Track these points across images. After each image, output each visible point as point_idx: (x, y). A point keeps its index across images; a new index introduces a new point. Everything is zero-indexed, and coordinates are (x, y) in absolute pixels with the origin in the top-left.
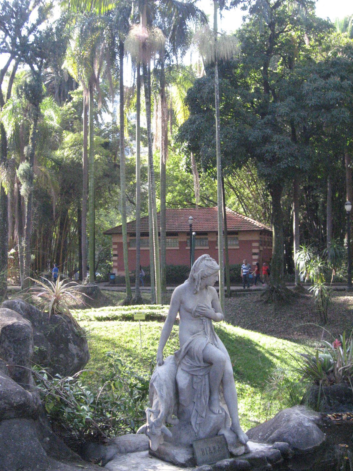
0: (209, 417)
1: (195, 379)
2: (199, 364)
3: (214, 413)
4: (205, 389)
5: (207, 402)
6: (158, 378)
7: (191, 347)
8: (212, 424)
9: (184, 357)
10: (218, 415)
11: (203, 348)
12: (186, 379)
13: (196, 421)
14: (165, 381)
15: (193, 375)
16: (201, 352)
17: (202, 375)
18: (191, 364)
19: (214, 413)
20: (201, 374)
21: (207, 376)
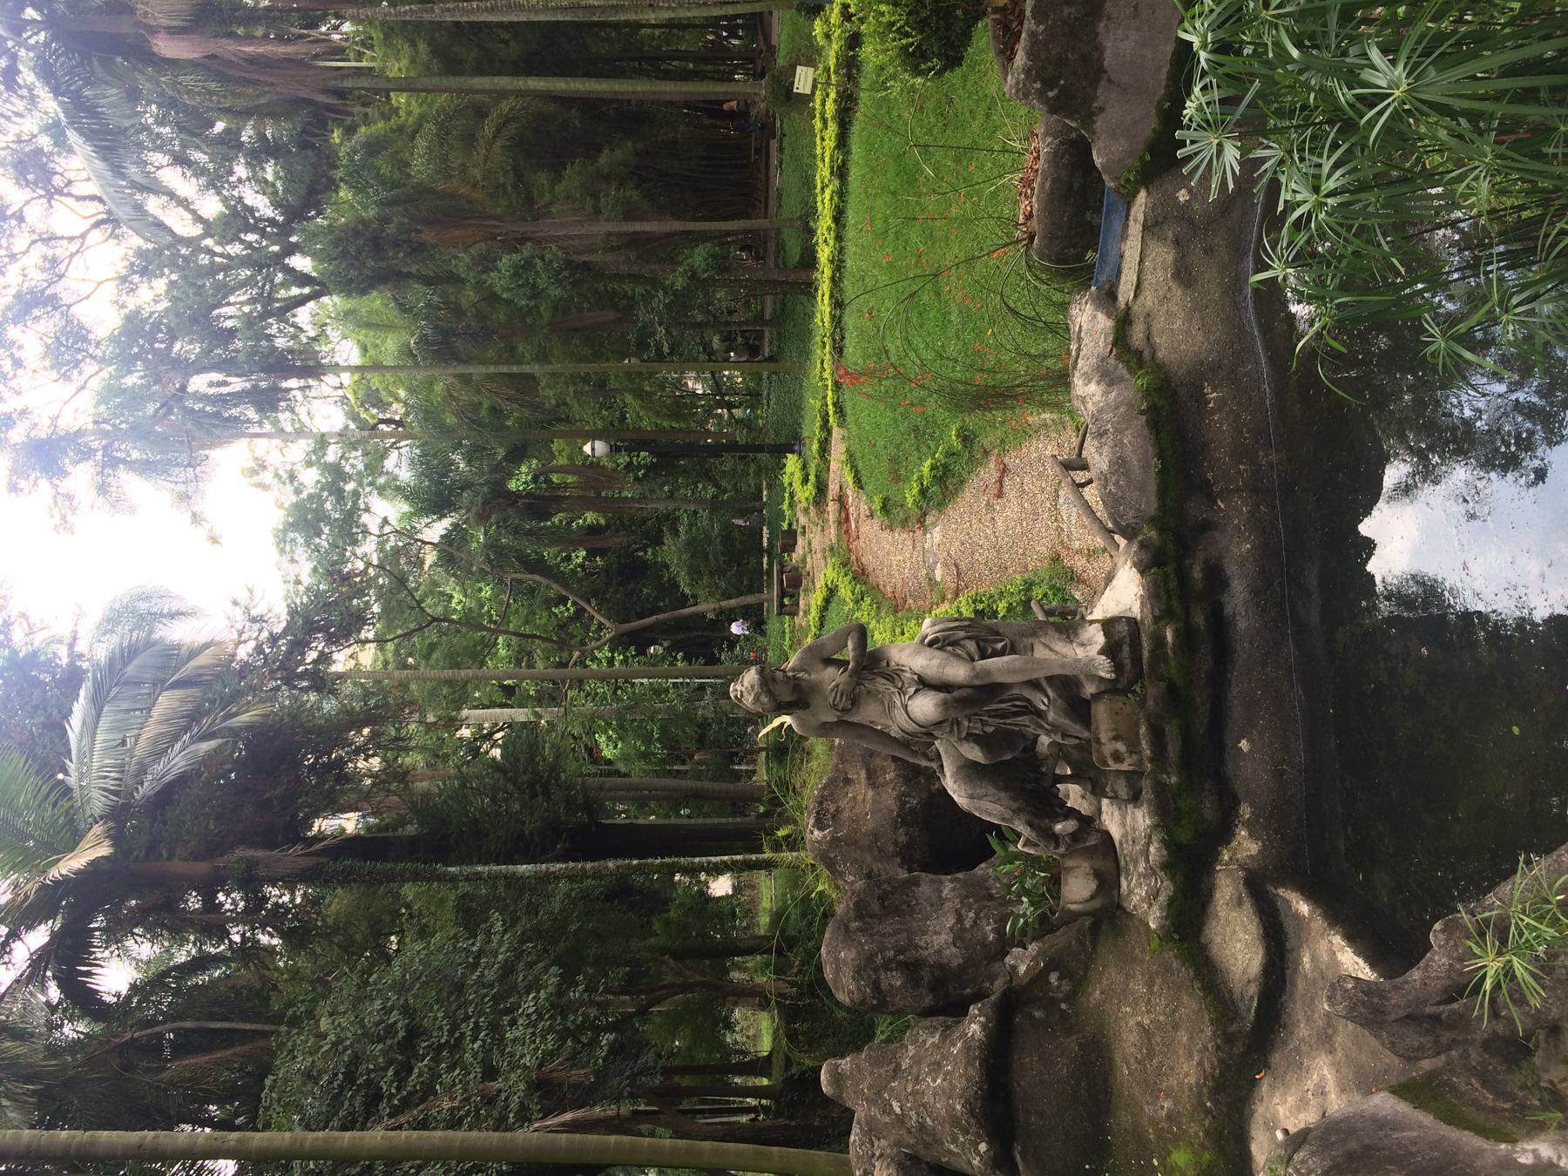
14: (971, 797)
15: (969, 735)
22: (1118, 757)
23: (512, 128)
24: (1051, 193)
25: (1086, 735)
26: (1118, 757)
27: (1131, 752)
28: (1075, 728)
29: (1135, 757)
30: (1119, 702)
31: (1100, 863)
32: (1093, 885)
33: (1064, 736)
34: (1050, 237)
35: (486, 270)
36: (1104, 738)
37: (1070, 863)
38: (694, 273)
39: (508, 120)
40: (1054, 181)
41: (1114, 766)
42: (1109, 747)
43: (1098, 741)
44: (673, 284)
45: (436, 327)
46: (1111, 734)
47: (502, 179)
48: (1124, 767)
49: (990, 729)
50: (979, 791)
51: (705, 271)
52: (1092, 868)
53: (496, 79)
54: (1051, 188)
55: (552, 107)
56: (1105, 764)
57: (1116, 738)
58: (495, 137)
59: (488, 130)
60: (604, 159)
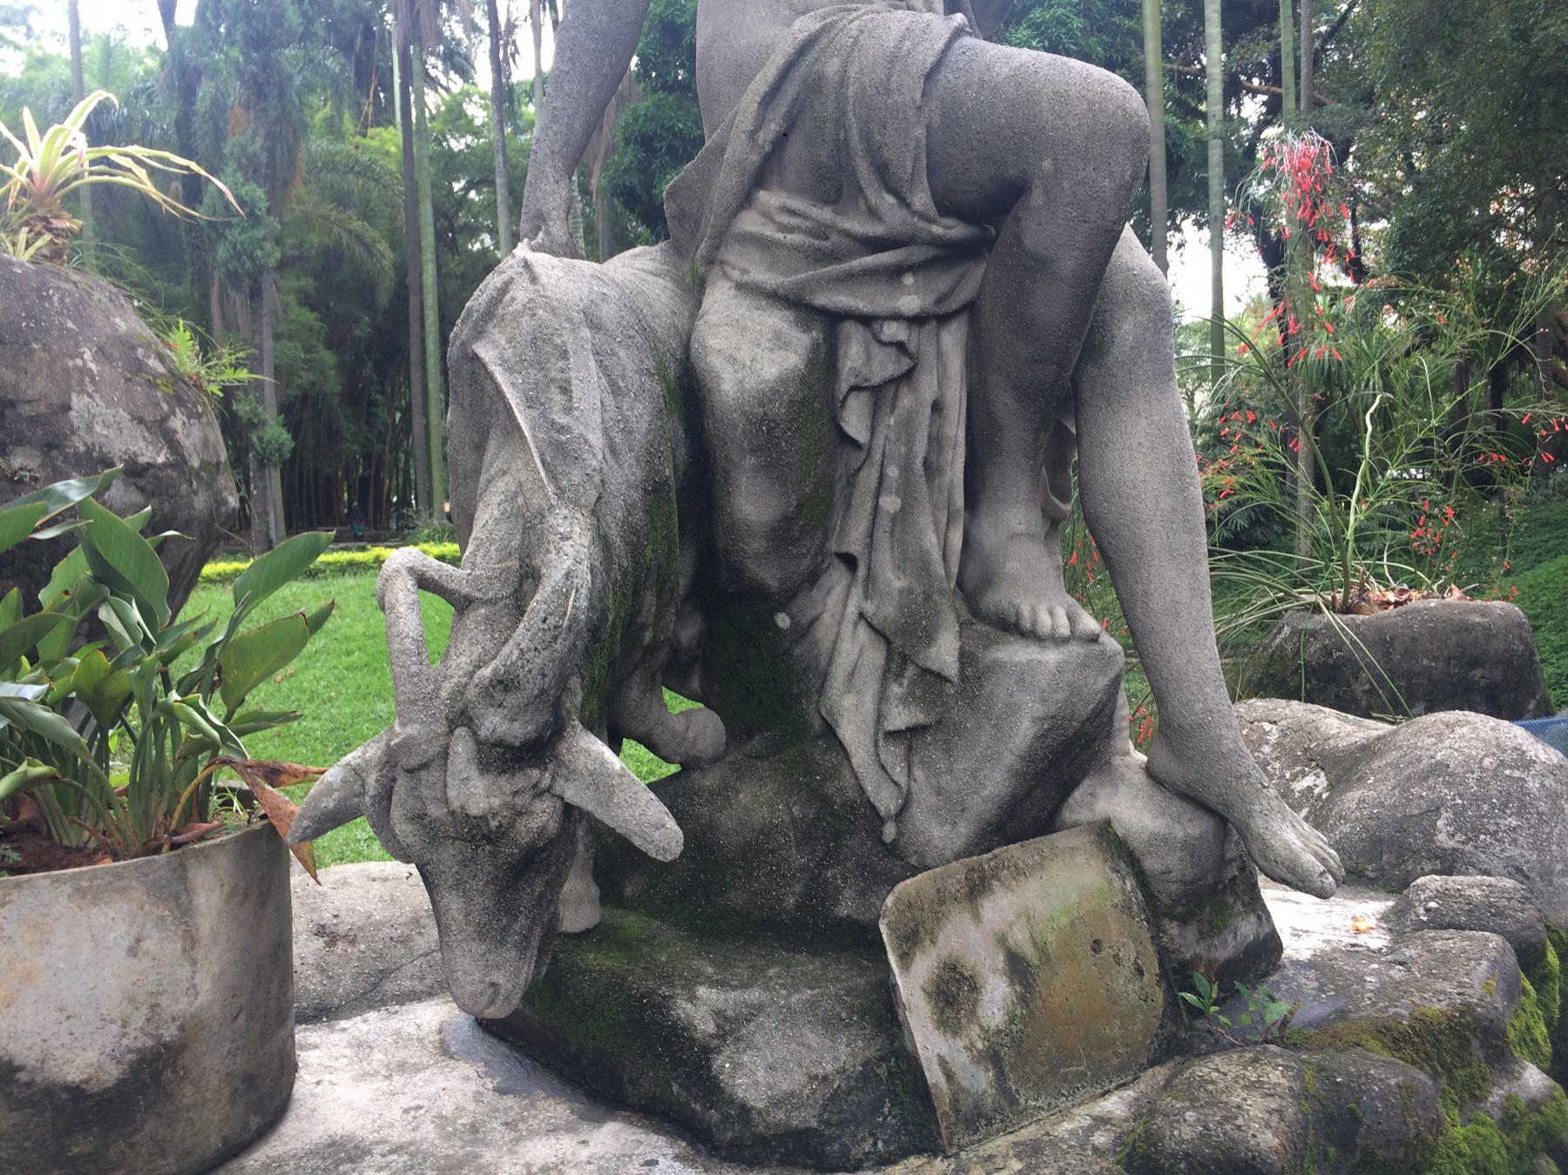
0: (997, 666)
1: (855, 354)
2: (893, 217)
3: (1032, 635)
4: (936, 442)
5: (955, 570)
6: (521, 293)
7: (815, 85)
8: (1024, 731)
9: (745, 201)
10: (1075, 650)
11: (926, 55)
12: (778, 341)
13: (880, 718)
15: (833, 320)
16: (912, 89)
17: (916, 321)
18: (820, 231)
19: (1032, 635)
20: (910, 303)
21: (953, 339)
22: (952, 994)
23: (359, 250)
24: (1468, 628)
25: (938, 832)
26: (952, 994)
27: (992, 1057)
28: (989, 772)
29: (980, 1080)
30: (1129, 943)
31: (213, 1065)
32: (84, 1057)
33: (909, 736)
34: (1383, 641)
35: (240, 167)
36: (999, 908)
37: (209, 892)
38: (254, 426)
39: (368, 247)
40: (1486, 629)
41: (912, 985)
42: (969, 938)
43: (977, 889)
44: (238, 401)
45: (120, 126)
46: (1020, 938)
47: (289, 242)
48: (928, 1041)
49: (855, 423)
50: (627, 360)
51: (261, 440)
52: (191, 1028)
53: (431, 229)
54: (1474, 626)
55: (383, 298)
56: (911, 941)
57: (1017, 966)
58: (350, 232)
59: (357, 225)
60: (329, 357)
